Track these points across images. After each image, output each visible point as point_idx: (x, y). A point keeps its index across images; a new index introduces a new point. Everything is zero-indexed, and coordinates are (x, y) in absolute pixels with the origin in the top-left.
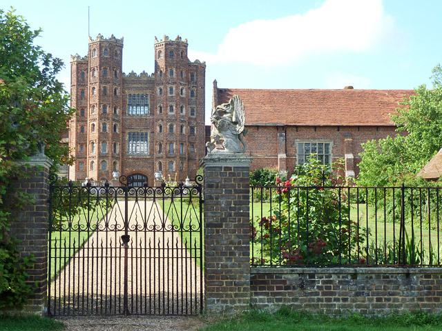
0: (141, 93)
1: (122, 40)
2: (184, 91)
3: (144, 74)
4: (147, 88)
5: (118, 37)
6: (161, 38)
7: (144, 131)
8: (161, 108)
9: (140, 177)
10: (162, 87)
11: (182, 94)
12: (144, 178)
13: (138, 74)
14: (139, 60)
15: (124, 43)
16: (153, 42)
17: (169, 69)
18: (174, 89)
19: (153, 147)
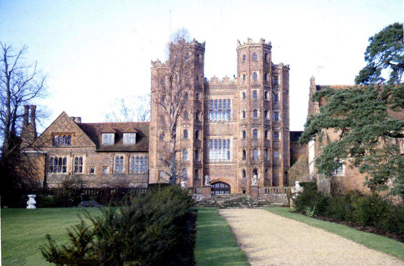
0: (223, 97)
1: (204, 44)
2: (268, 95)
3: (225, 79)
4: (229, 94)
5: (200, 41)
6: (244, 40)
7: (226, 138)
8: (244, 112)
9: (222, 186)
10: (245, 91)
11: (266, 98)
12: (226, 186)
13: (220, 78)
14: (220, 66)
15: (206, 47)
16: (235, 46)
17: (253, 72)
18: (258, 92)
19: (236, 153)
